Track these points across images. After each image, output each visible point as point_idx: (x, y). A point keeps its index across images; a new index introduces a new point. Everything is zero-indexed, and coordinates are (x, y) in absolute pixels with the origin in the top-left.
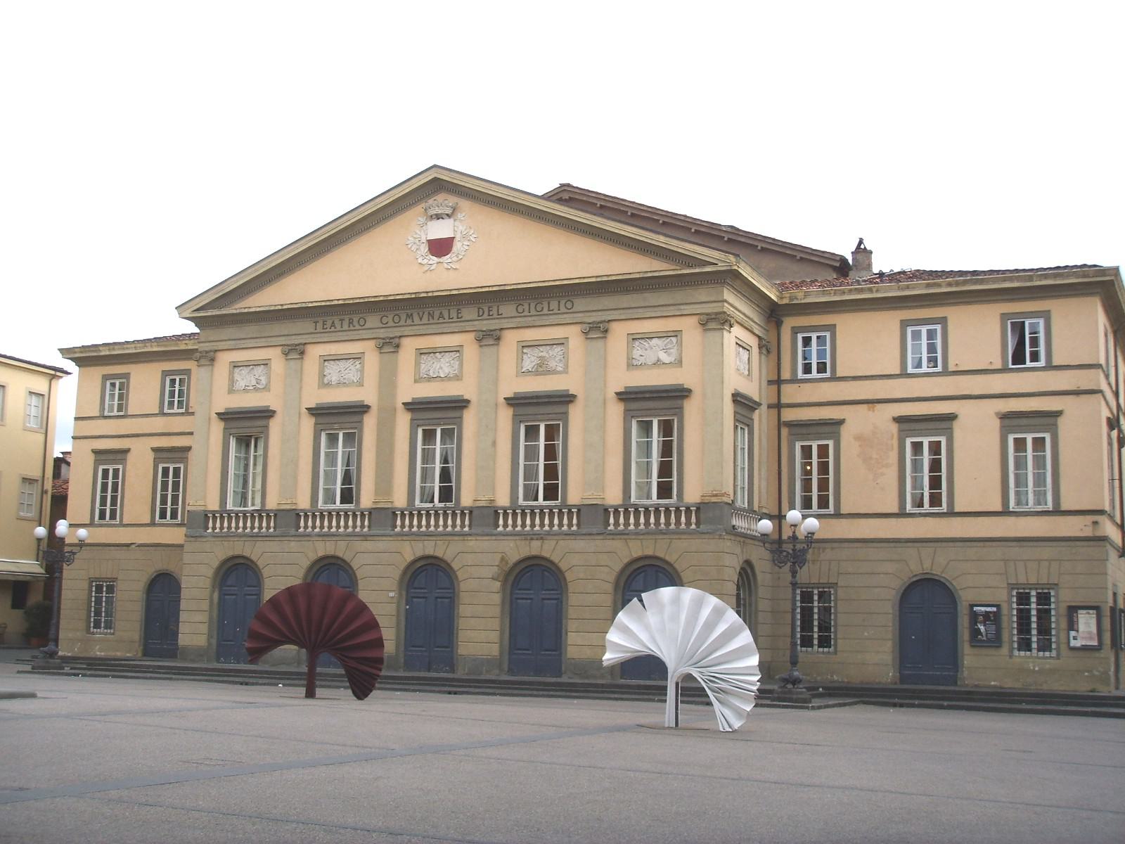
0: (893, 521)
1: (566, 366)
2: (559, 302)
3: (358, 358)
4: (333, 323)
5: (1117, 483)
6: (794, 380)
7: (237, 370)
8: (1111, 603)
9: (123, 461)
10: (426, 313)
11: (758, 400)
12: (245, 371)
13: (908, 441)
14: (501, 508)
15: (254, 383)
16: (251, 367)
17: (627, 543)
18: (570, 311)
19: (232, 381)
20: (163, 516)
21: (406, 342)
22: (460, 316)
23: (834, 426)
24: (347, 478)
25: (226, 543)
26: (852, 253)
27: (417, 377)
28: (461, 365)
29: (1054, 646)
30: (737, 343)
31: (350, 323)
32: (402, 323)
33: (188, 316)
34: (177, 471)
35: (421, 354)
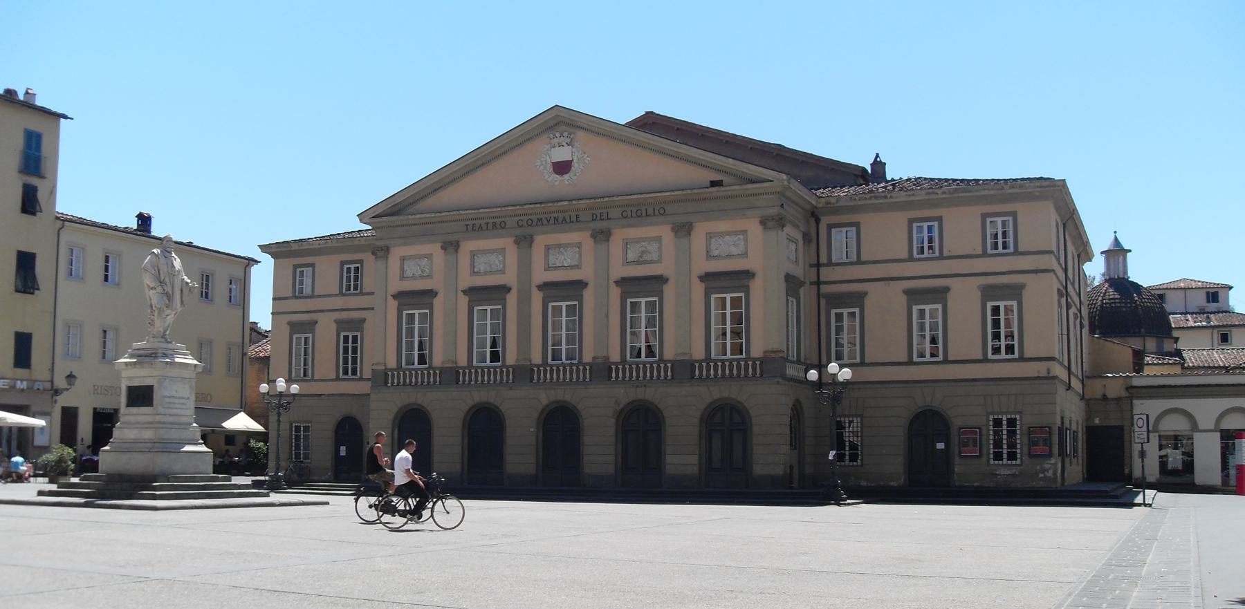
0: (904, 367)
1: (660, 256)
4: (481, 225)
5: (1065, 337)
6: (830, 264)
8: (1059, 423)
9: (312, 331)
10: (552, 218)
11: (803, 280)
13: (915, 308)
15: (420, 272)
19: (402, 270)
20: (346, 373)
23: (857, 299)
24: (494, 344)
26: (871, 164)
28: (580, 256)
29: (1019, 456)
30: (787, 239)
33: (367, 221)
34: (355, 338)
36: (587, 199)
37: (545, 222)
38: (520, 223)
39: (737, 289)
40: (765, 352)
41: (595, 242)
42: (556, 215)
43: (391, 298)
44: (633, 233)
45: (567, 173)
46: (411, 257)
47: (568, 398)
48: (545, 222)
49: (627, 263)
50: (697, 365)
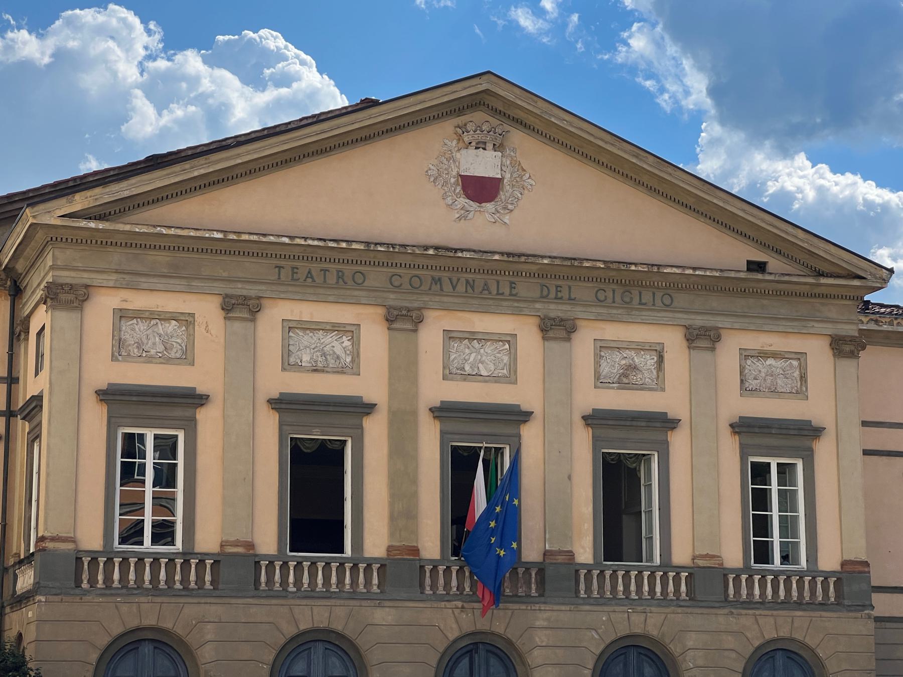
2: (654, 294)
3: (351, 331)
7: (126, 325)
10: (463, 281)
12: (141, 326)
14: (265, 557)
15: (161, 348)
16: (153, 322)
18: (668, 307)
22: (514, 292)
25: (124, 608)
27: (447, 372)
31: (338, 277)
32: (425, 287)
35: (450, 338)
36: (474, 251)
37: (447, 287)
39: (795, 452)
40: (844, 564)
41: (544, 338)
43: (94, 397)
44: (613, 332)
45: (490, 201)
47: (499, 627)
48: (447, 287)
49: (600, 381)
50: (731, 577)
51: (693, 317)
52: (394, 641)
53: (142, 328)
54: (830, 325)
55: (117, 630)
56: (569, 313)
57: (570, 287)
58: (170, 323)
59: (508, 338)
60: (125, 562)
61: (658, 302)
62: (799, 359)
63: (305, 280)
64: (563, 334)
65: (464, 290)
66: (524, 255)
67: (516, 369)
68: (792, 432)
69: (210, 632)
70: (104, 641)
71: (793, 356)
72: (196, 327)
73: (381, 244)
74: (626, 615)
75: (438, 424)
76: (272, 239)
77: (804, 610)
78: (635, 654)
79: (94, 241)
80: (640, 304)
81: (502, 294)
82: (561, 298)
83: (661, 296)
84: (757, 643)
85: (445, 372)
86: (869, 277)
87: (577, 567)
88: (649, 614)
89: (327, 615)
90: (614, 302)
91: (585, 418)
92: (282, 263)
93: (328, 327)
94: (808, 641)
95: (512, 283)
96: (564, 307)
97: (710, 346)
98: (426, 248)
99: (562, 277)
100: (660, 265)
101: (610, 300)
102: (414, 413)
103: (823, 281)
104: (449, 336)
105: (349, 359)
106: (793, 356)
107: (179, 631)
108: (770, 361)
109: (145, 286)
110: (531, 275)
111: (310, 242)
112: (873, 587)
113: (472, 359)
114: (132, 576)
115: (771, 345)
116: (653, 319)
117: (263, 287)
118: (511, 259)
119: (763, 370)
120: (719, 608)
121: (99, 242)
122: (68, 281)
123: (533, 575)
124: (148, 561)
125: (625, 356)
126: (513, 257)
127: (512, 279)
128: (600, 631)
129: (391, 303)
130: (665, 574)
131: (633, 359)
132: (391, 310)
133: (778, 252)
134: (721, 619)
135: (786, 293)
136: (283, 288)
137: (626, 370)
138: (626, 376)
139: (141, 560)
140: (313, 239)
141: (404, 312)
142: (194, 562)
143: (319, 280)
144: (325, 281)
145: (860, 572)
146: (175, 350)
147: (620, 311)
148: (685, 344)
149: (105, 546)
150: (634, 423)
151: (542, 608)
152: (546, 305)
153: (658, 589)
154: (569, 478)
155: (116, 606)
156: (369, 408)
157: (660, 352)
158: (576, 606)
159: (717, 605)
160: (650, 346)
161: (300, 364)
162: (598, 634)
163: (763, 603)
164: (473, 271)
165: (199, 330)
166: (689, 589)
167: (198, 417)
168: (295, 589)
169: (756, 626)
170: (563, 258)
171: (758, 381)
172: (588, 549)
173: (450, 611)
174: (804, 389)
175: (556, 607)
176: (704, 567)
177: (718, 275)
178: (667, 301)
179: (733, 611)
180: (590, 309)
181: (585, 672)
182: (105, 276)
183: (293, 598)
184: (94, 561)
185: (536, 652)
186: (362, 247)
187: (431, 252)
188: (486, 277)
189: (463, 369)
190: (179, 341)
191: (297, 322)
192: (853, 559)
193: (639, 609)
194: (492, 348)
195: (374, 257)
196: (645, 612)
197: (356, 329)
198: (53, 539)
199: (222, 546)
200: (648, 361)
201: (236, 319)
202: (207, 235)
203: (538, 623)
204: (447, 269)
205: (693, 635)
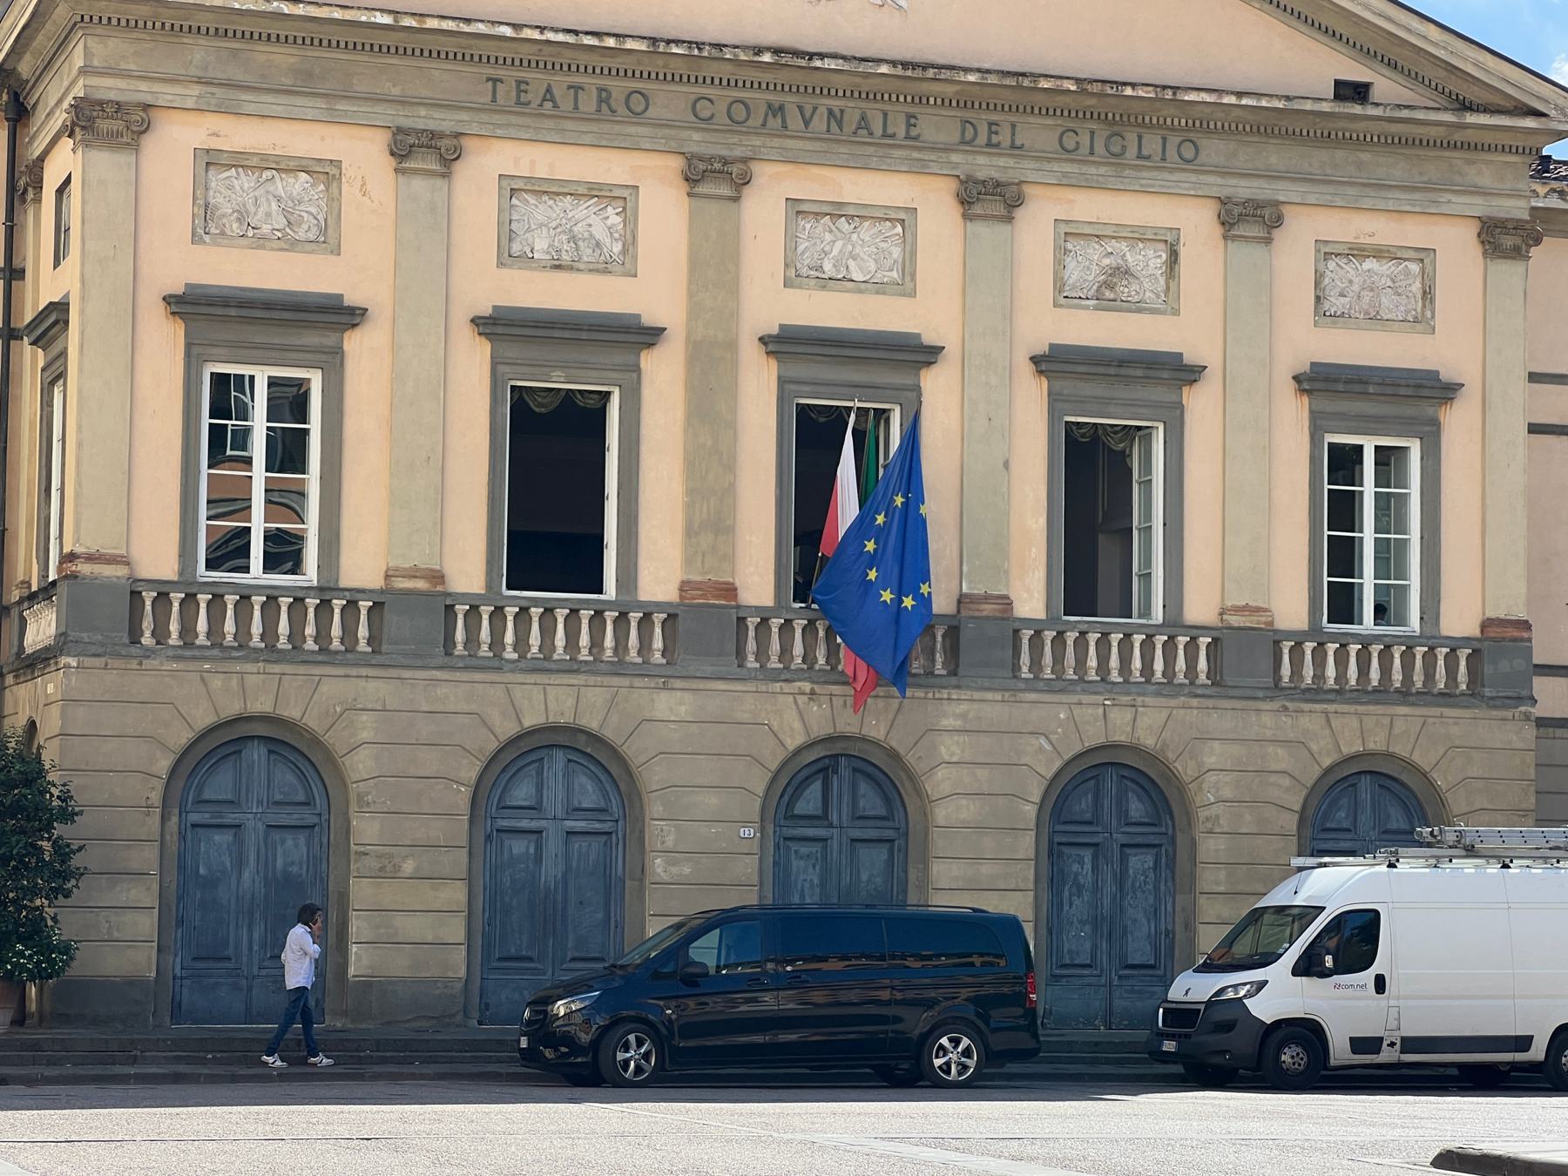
2: (1164, 139)
3: (623, 198)
4: (549, 90)
7: (217, 179)
10: (823, 110)
12: (244, 182)
16: (267, 174)
17: (1328, 721)
18: (1189, 163)
21: (764, 172)
22: (914, 132)
25: (217, 682)
27: (792, 273)
31: (600, 101)
32: (755, 122)
35: (798, 212)
36: (844, 58)
37: (795, 122)
38: (705, 109)
39: (1407, 426)
40: (1486, 624)
41: (966, 217)
42: (836, 104)
44: (1090, 206)
46: (239, 161)
47: (875, 728)
48: (795, 122)
49: (1064, 296)
50: (1286, 646)
51: (1233, 182)
52: (690, 750)
53: (246, 186)
54: (1478, 200)
55: (204, 718)
56: (1010, 171)
57: (1013, 126)
58: (296, 178)
59: (902, 215)
60: (217, 600)
61: (1172, 153)
62: (1422, 260)
63: (541, 105)
64: (1000, 209)
65: (825, 128)
66: (933, 66)
67: (915, 271)
68: (1402, 391)
69: (366, 727)
70: (181, 737)
71: (1411, 254)
72: (345, 187)
73: (677, 42)
74: (1101, 710)
75: (773, 364)
76: (481, 28)
77: (1413, 704)
78: (1114, 778)
79: (158, 25)
80: (1140, 157)
81: (893, 136)
82: (997, 145)
83: (1177, 144)
84: (1327, 762)
85: (787, 274)
86: (1553, 113)
87: (1017, 625)
88: (1140, 709)
89: (571, 702)
90: (1092, 153)
91: (1035, 360)
92: (500, 72)
93: (581, 190)
94: (1417, 758)
95: (910, 116)
96: (1002, 162)
97: (1262, 235)
98: (759, 51)
99: (999, 108)
100: (1178, 88)
101: (1085, 149)
102: (732, 346)
103: (1471, 118)
104: (797, 209)
105: (617, 248)
106: (1411, 254)
107: (312, 722)
108: (1370, 264)
109: (250, 108)
110: (945, 103)
111: (551, 36)
112: (1536, 666)
113: (835, 252)
114: (229, 626)
115: (1372, 235)
116: (1161, 186)
117: (465, 116)
118: (909, 73)
119: (1356, 280)
120: (1264, 699)
121: (168, 26)
122: (112, 96)
123: (939, 639)
124: (258, 600)
125: (1110, 250)
126: (914, 69)
127: (911, 110)
128: (1053, 737)
129: (695, 149)
130: (1172, 638)
131: (1124, 255)
132: (695, 161)
133: (1392, 65)
134: (1267, 719)
135: (1403, 140)
136: (496, 118)
137: (1110, 275)
138: (1112, 288)
139: (245, 598)
140: (555, 30)
141: (717, 166)
142: (338, 604)
143: (566, 105)
144: (576, 107)
145: (1514, 640)
146: (305, 227)
147: (1102, 170)
148: (1218, 230)
149: (181, 573)
150: (1123, 371)
151: (953, 697)
152: (970, 158)
153: (1159, 665)
154: (1006, 465)
155: (202, 679)
156: (651, 336)
157: (1172, 245)
158: (1012, 692)
159: (1261, 694)
160: (1155, 234)
161: (530, 255)
162: (1051, 743)
163: (1339, 692)
164: (841, 93)
165: (349, 191)
166: (1212, 666)
167: (346, 347)
168: (515, 656)
169: (1327, 731)
170: (1002, 72)
171: (1347, 299)
172: (1036, 595)
173: (791, 699)
174: (1429, 314)
175: (977, 695)
176: (1240, 628)
177: (1281, 106)
178: (1188, 152)
179: (1288, 704)
180: (1048, 166)
181: (1027, 808)
182: (178, 89)
183: (512, 671)
184: (162, 598)
185: (940, 773)
186: (642, 46)
187: (767, 58)
188: (863, 105)
189: (820, 268)
190: (313, 210)
191: (525, 180)
192: (1502, 617)
193: (1125, 699)
194: (872, 232)
195: (665, 66)
196: (1134, 706)
197: (631, 194)
198: (91, 558)
199: (387, 577)
200: (1149, 261)
201: (415, 172)
202: (364, 19)
203: (948, 722)
204: (794, 89)
205: (1216, 744)
